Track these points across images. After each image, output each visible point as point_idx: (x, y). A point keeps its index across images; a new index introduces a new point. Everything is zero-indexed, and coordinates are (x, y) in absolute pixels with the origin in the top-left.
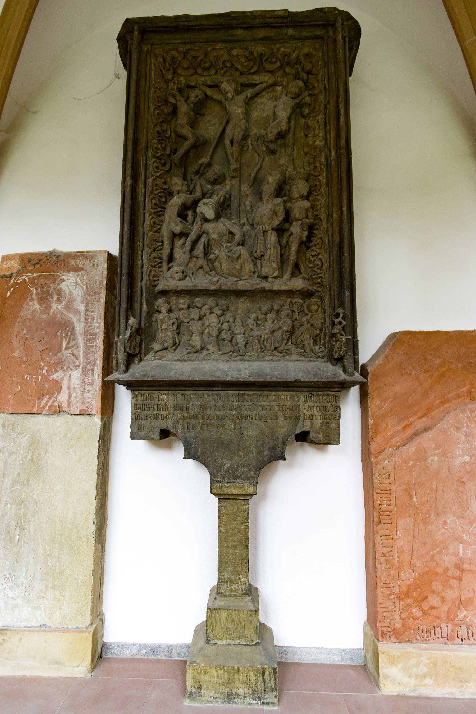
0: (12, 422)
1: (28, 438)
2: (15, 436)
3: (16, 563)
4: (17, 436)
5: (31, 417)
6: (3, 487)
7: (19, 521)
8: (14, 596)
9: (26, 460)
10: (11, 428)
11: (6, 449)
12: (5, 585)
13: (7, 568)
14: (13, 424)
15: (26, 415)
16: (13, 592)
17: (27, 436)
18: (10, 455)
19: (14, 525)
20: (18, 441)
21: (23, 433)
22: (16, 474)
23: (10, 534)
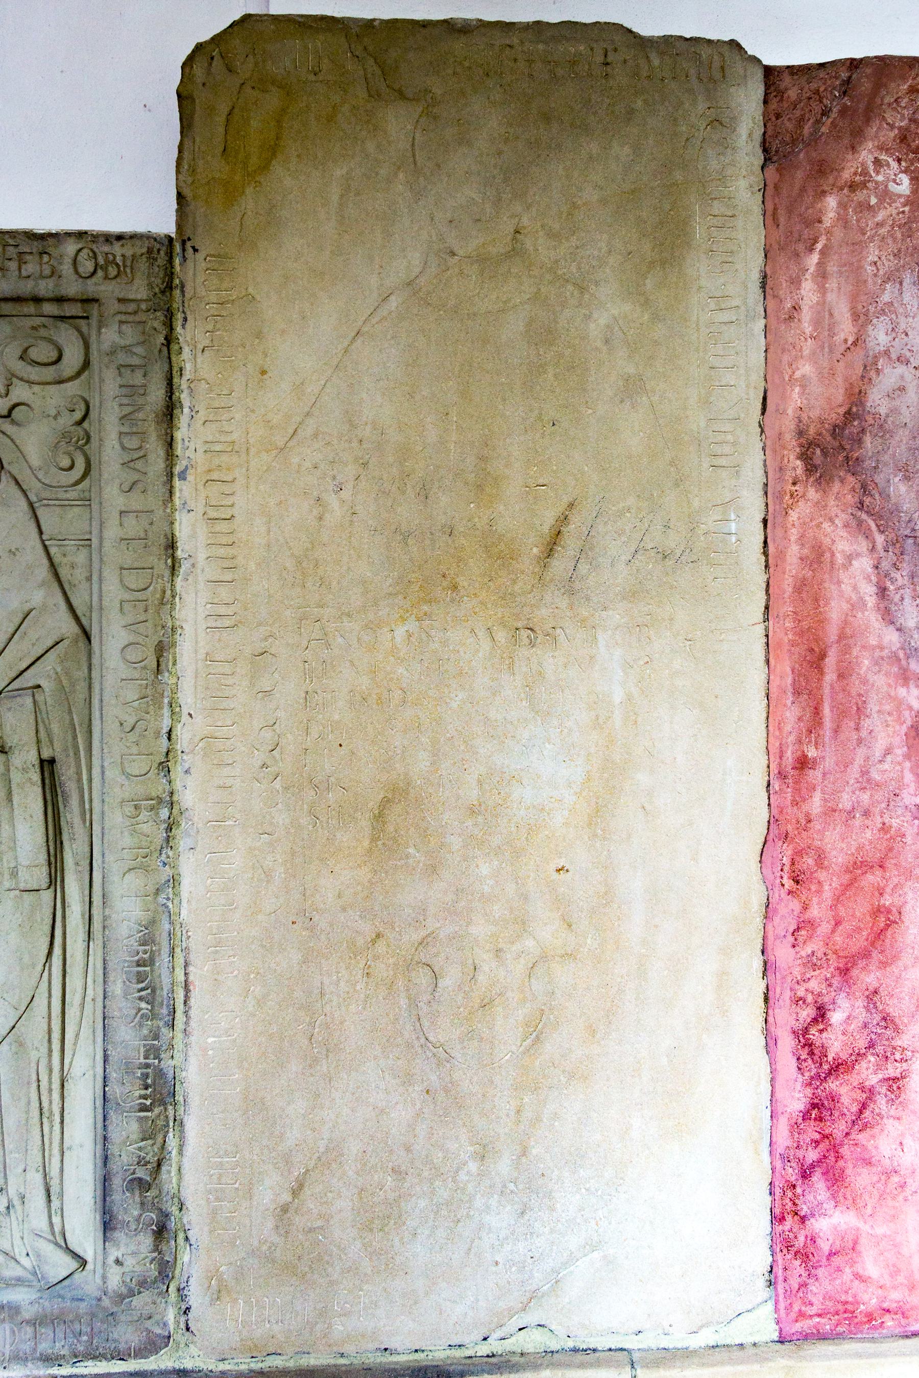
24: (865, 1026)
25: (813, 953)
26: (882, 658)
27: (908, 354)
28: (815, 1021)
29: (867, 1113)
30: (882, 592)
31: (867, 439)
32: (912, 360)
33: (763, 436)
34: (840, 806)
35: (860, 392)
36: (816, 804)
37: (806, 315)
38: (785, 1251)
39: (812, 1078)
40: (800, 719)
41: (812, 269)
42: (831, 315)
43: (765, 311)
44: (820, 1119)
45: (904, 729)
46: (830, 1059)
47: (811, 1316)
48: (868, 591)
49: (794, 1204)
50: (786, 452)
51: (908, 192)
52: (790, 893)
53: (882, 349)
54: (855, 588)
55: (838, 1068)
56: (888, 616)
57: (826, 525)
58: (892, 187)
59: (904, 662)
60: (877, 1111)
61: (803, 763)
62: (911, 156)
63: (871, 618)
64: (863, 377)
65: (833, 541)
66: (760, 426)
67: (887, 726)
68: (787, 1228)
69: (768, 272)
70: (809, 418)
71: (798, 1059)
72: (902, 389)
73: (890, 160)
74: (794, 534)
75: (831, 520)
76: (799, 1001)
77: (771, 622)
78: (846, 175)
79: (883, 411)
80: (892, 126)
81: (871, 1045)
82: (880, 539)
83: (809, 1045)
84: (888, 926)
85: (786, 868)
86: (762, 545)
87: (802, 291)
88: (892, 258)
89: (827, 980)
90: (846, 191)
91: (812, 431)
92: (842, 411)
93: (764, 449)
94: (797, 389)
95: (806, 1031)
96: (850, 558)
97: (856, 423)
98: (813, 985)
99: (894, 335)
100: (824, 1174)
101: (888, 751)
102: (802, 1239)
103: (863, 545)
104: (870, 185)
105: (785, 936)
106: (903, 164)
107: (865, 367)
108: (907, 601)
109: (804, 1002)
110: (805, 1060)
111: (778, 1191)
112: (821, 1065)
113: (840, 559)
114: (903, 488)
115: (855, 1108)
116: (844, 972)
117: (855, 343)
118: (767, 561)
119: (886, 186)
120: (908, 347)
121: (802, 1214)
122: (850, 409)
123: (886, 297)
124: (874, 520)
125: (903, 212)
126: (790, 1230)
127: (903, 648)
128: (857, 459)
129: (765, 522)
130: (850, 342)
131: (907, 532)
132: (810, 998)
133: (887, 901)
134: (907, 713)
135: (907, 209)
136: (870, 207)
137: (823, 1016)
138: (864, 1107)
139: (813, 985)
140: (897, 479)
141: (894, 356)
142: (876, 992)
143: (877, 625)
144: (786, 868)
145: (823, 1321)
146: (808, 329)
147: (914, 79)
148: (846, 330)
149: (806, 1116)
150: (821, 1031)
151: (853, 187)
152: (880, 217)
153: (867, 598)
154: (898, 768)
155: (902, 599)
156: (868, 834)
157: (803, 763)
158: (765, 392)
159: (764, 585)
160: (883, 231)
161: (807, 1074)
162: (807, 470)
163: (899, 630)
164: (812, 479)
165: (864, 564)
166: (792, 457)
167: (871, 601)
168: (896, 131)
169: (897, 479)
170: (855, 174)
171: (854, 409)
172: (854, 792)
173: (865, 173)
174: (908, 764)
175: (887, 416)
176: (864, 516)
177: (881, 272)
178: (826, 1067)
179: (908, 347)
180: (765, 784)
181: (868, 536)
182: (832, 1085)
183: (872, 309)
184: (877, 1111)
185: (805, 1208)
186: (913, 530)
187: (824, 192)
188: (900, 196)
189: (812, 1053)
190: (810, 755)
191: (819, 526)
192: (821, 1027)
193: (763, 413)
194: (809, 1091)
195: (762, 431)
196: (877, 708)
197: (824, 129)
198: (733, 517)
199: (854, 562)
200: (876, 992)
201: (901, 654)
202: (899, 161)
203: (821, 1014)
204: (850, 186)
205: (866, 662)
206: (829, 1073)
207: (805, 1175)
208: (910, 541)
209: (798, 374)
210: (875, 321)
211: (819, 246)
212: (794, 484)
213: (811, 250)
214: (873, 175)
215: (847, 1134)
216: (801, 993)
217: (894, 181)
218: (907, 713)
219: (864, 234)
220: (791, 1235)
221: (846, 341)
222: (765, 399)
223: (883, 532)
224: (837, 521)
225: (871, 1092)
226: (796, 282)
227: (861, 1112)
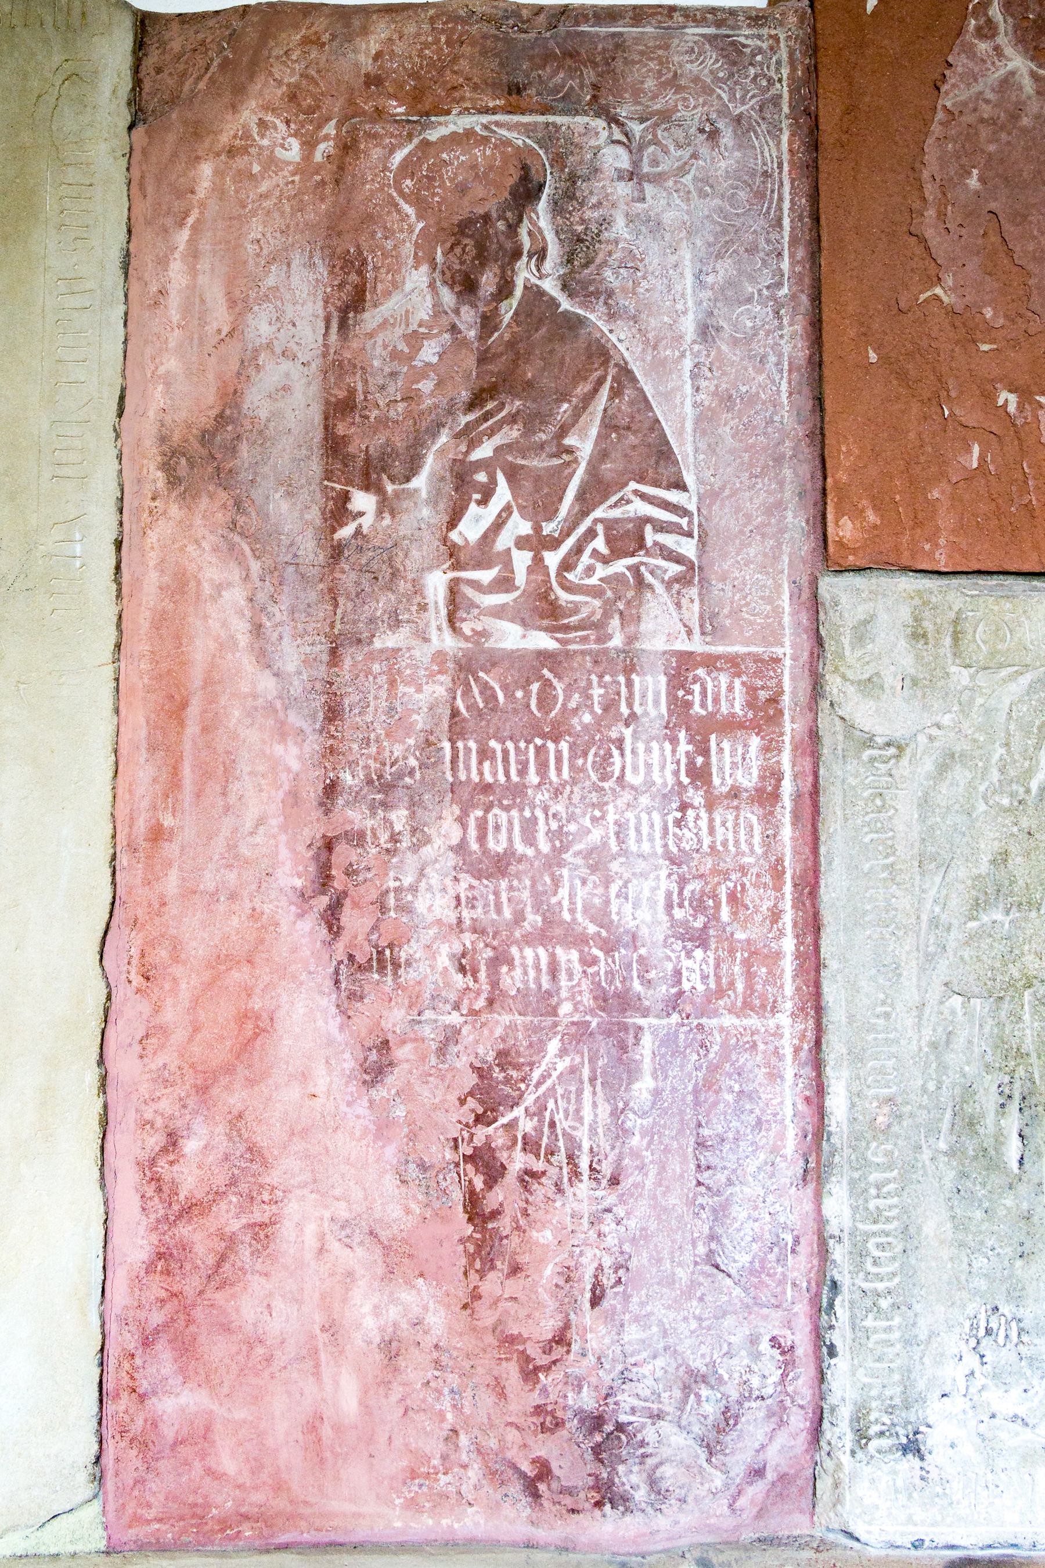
0: (952, 615)
1: (1031, 689)
2: (965, 681)
3: (1019, 1263)
4: (972, 677)
5: (1035, 589)
6: (924, 917)
7: (1021, 1072)
8: (1021, 1412)
9: (1028, 791)
10: (948, 641)
11: (922, 739)
12: (972, 1361)
13: (982, 1284)
14: (956, 622)
15: (1010, 581)
16: (1016, 1392)
17: (1025, 680)
18: (943, 768)
19: (994, 1088)
20: (980, 701)
21: (1001, 666)
22: (985, 859)
23: (982, 1131)
24: (226, 1158)
25: (165, 1065)
26: (256, 709)
27: (295, 348)
28: (164, 1150)
29: (227, 1266)
30: (257, 629)
31: (244, 448)
32: (299, 355)
33: (119, 444)
34: (202, 887)
35: (235, 392)
36: (171, 883)
37: (174, 301)
38: (118, 1437)
39: (158, 1221)
40: (155, 780)
41: (181, 248)
42: (203, 301)
43: (126, 296)
44: (168, 1272)
45: (281, 794)
46: (182, 1197)
47: (148, 1522)
48: (241, 628)
49: (132, 1378)
50: (145, 462)
51: (298, 159)
52: (138, 991)
53: (264, 341)
54: (224, 624)
55: (190, 1210)
56: (264, 659)
57: (190, 548)
58: (279, 153)
59: (281, 714)
60: (239, 1264)
61: (157, 834)
62: (302, 117)
63: (247, 663)
64: (239, 374)
65: (200, 568)
66: (115, 430)
67: (261, 790)
68: (122, 1408)
69: (132, 250)
70: (174, 421)
71: (143, 1197)
72: (286, 388)
73: (278, 122)
74: (153, 558)
75: (197, 542)
76: (145, 1124)
77: (123, 664)
78: (224, 139)
79: (263, 414)
80: (279, 83)
81: (233, 1182)
82: (255, 566)
83: (156, 1179)
84: (256, 1035)
85: (134, 962)
86: (113, 571)
87: (170, 273)
88: (278, 235)
89: (181, 1099)
90: (223, 157)
91: (176, 437)
92: (213, 413)
93: (120, 457)
94: (160, 388)
95: (153, 1162)
96: (219, 588)
97: (229, 428)
98: (164, 1105)
99: (279, 325)
100: (170, 1341)
101: (261, 821)
102: (140, 1422)
103: (235, 574)
104: (252, 150)
105: (130, 1045)
106: (293, 126)
107: (243, 362)
108: (286, 640)
109: (152, 1127)
110: (151, 1198)
111: (112, 1363)
112: (170, 1204)
113: (207, 589)
114: (285, 506)
115: (211, 1260)
116: (202, 1090)
117: (230, 334)
118: (119, 591)
119: (272, 152)
120: (296, 339)
121: (141, 1391)
122: (223, 411)
123: (271, 281)
124: (249, 544)
125: (293, 182)
126: (126, 1412)
127: (280, 697)
128: (231, 471)
129: (119, 544)
130: (224, 333)
131: (288, 558)
132: (159, 1122)
133: (256, 1004)
134: (284, 776)
135: (297, 178)
136: (252, 176)
137: (174, 1144)
138: (222, 1258)
139: (164, 1105)
140: (277, 496)
141: (278, 350)
142: (240, 1116)
143: (250, 668)
144: (134, 962)
145: (164, 1527)
146: (175, 317)
147: (308, 28)
148: (220, 317)
149: (150, 1268)
150: (172, 1163)
151: (231, 152)
152: (263, 188)
153: (239, 637)
154: (272, 842)
155: (281, 638)
156: (235, 921)
157: (157, 834)
158: (123, 390)
159: (115, 619)
160: (268, 204)
161: (153, 1216)
162: (169, 482)
163: (276, 675)
164: (174, 494)
165: (236, 596)
166: (152, 468)
167: (243, 639)
168: (285, 88)
169: (277, 496)
170: (235, 137)
171: (228, 412)
172: (218, 871)
173: (247, 135)
174: (283, 838)
175: (268, 420)
176: (237, 538)
177: (265, 252)
178: (176, 1207)
179: (296, 339)
180: (108, 858)
181: (241, 562)
182: (184, 1230)
183: (253, 295)
184: (239, 1264)
185: (145, 1383)
186: (295, 556)
187: (198, 158)
188: (288, 163)
189: (159, 1190)
190: (166, 824)
191: (182, 549)
192: (172, 1157)
193: (120, 415)
194: (154, 1238)
195: (118, 437)
196: (249, 769)
197: (202, 85)
198: (78, 537)
199: (224, 593)
200: (240, 1116)
201: (278, 705)
202: (288, 123)
203: (173, 1141)
204: (229, 152)
205: (237, 713)
206: (179, 1217)
207: (147, 1343)
208: (291, 569)
209: (162, 370)
210: (256, 308)
211: (190, 220)
212: (154, 499)
213: (181, 224)
214: (257, 138)
215: (201, 1293)
216: (148, 1115)
217: (282, 146)
218: (284, 776)
219: (244, 207)
220: (127, 1418)
221: (219, 331)
222: (122, 398)
223: (258, 558)
224: (204, 544)
225: (231, 1241)
226: (163, 262)
227: (218, 1265)
